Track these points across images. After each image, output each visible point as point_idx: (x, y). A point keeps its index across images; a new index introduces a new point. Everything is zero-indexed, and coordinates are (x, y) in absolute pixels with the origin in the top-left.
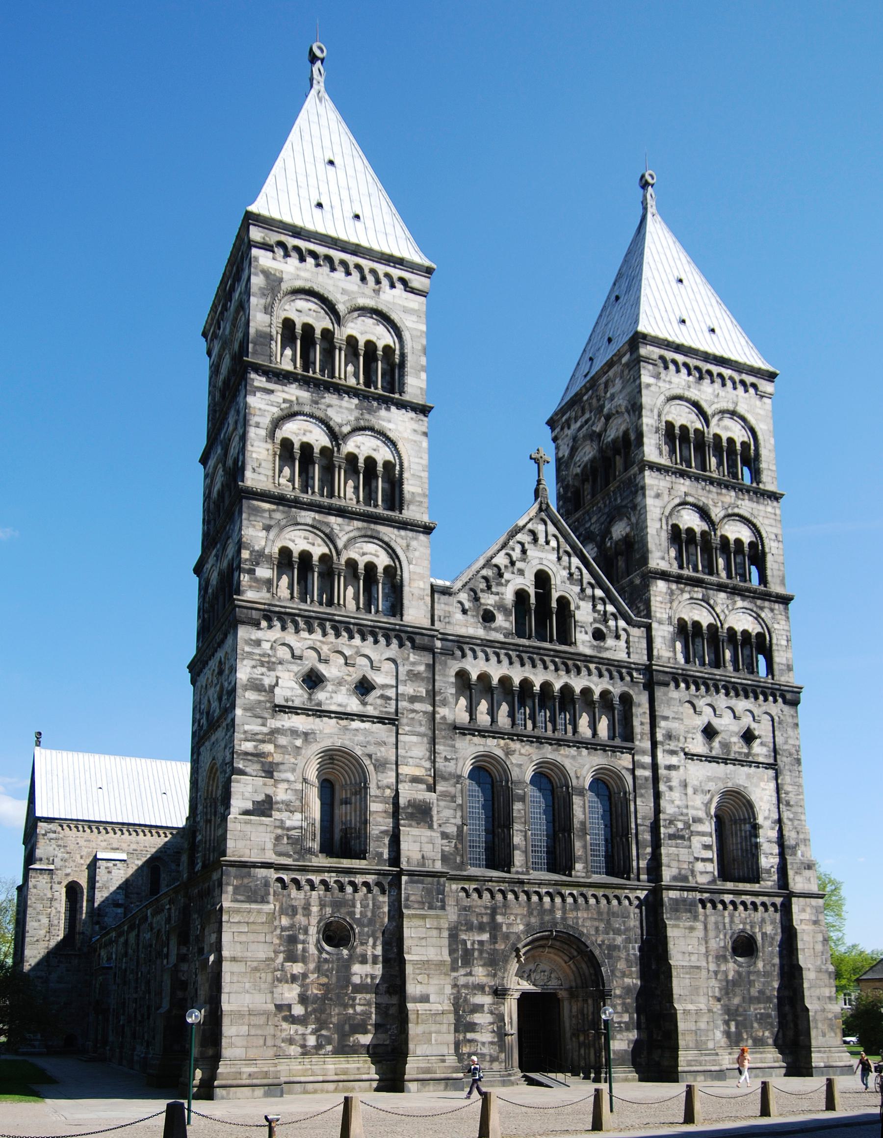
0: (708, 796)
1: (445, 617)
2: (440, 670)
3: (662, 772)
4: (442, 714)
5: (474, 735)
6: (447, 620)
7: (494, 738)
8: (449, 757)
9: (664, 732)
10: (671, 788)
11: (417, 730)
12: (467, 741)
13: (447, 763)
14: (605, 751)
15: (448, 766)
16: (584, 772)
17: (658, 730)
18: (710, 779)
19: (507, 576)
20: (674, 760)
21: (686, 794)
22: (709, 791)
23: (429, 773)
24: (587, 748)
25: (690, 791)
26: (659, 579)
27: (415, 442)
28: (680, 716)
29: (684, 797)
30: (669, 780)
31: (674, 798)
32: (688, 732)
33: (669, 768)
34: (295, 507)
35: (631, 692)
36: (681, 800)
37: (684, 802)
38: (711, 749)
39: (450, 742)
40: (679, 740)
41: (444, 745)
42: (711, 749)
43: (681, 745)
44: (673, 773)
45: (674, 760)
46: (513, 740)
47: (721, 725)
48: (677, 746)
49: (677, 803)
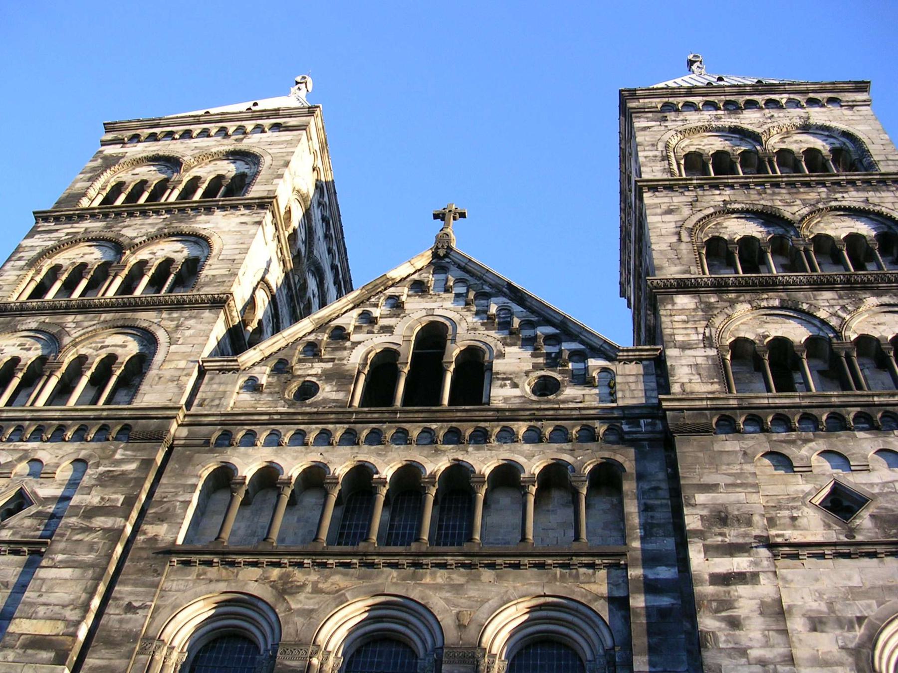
0: (859, 632)
1: (213, 400)
2: (172, 470)
3: (705, 589)
4: (150, 535)
5: (210, 563)
6: (217, 402)
7: (255, 564)
8: (136, 604)
9: (705, 512)
10: (734, 623)
11: (81, 558)
12: (193, 577)
13: (129, 616)
14: (541, 566)
15: (128, 621)
16: (481, 615)
17: (686, 511)
18: (855, 593)
19: (354, 338)
20: (740, 563)
21: (785, 632)
22: (860, 620)
23: (71, 629)
24: (492, 566)
25: (797, 624)
26: (678, 293)
27: (239, 232)
28: (751, 480)
29: (775, 637)
30: (726, 604)
31: (745, 642)
32: (778, 507)
33: (726, 579)
34: (21, 315)
35: (619, 458)
36: (767, 645)
37: (782, 650)
38: (851, 533)
39: (150, 579)
40: (749, 523)
41: (135, 584)
42: (851, 533)
43: (756, 532)
44: (742, 590)
45: (740, 563)
46: (300, 565)
47: (872, 485)
48: (745, 535)
49: (754, 653)
